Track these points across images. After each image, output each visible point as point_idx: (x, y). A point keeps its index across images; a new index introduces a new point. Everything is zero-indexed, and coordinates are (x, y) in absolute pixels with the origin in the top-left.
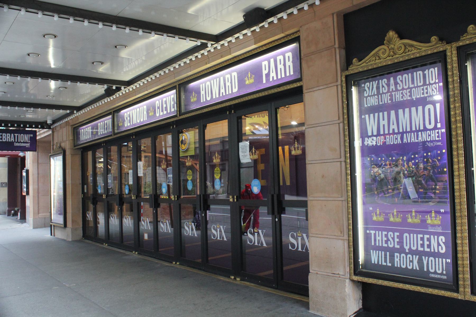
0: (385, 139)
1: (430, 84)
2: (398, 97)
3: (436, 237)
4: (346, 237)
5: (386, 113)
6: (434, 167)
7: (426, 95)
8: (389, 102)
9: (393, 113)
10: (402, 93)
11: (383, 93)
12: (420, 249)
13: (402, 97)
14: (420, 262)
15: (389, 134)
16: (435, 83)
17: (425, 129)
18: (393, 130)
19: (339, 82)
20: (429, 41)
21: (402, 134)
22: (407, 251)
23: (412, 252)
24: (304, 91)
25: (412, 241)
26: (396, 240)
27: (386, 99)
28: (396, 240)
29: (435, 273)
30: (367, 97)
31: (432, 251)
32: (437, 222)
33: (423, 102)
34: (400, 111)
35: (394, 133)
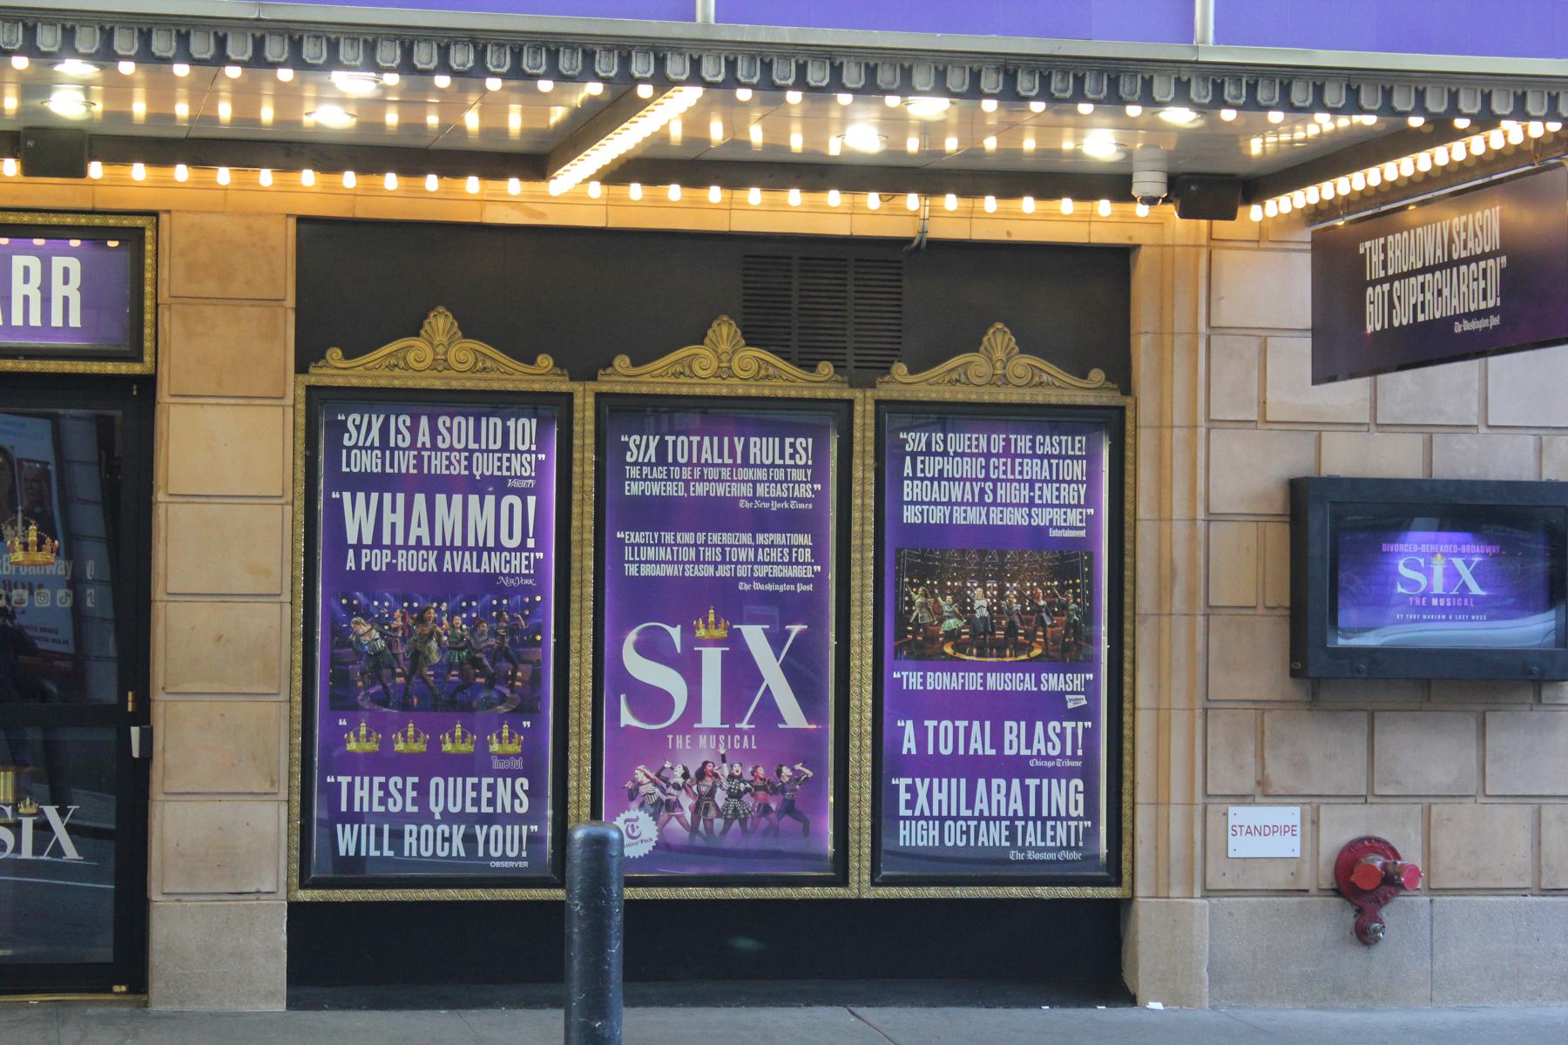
0: (394, 556)
1: (517, 451)
2: (438, 464)
3: (509, 780)
4: (284, 794)
5: (400, 497)
6: (513, 630)
7: (505, 473)
8: (412, 471)
9: (420, 500)
10: (448, 458)
11: (397, 448)
12: (470, 809)
13: (448, 468)
14: (469, 839)
15: (406, 547)
16: (529, 451)
17: (499, 547)
18: (419, 539)
19: (289, 400)
20: (531, 361)
21: (441, 551)
22: (438, 817)
23: (447, 817)
24: (163, 395)
25: (449, 794)
26: (411, 794)
27: (405, 463)
28: (411, 794)
29: (504, 857)
30: (349, 449)
31: (499, 810)
32: (514, 748)
33: (499, 486)
34: (441, 499)
35: (419, 546)
